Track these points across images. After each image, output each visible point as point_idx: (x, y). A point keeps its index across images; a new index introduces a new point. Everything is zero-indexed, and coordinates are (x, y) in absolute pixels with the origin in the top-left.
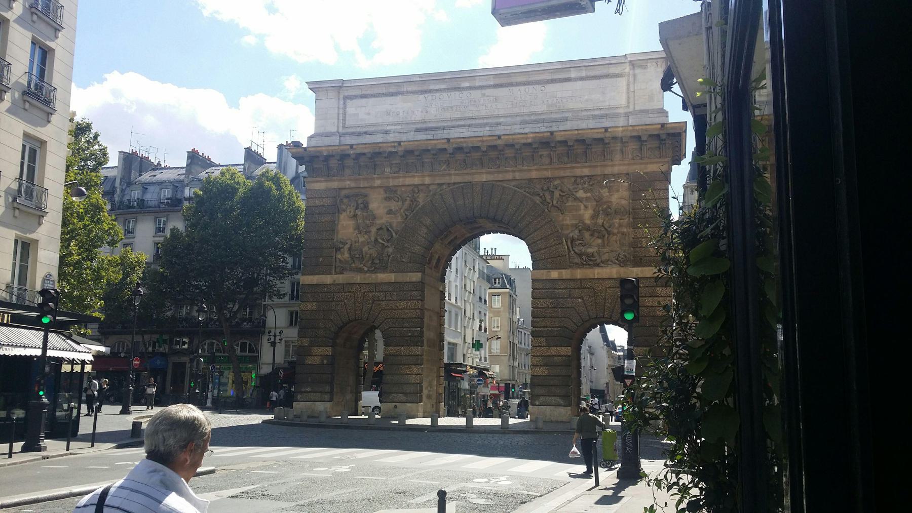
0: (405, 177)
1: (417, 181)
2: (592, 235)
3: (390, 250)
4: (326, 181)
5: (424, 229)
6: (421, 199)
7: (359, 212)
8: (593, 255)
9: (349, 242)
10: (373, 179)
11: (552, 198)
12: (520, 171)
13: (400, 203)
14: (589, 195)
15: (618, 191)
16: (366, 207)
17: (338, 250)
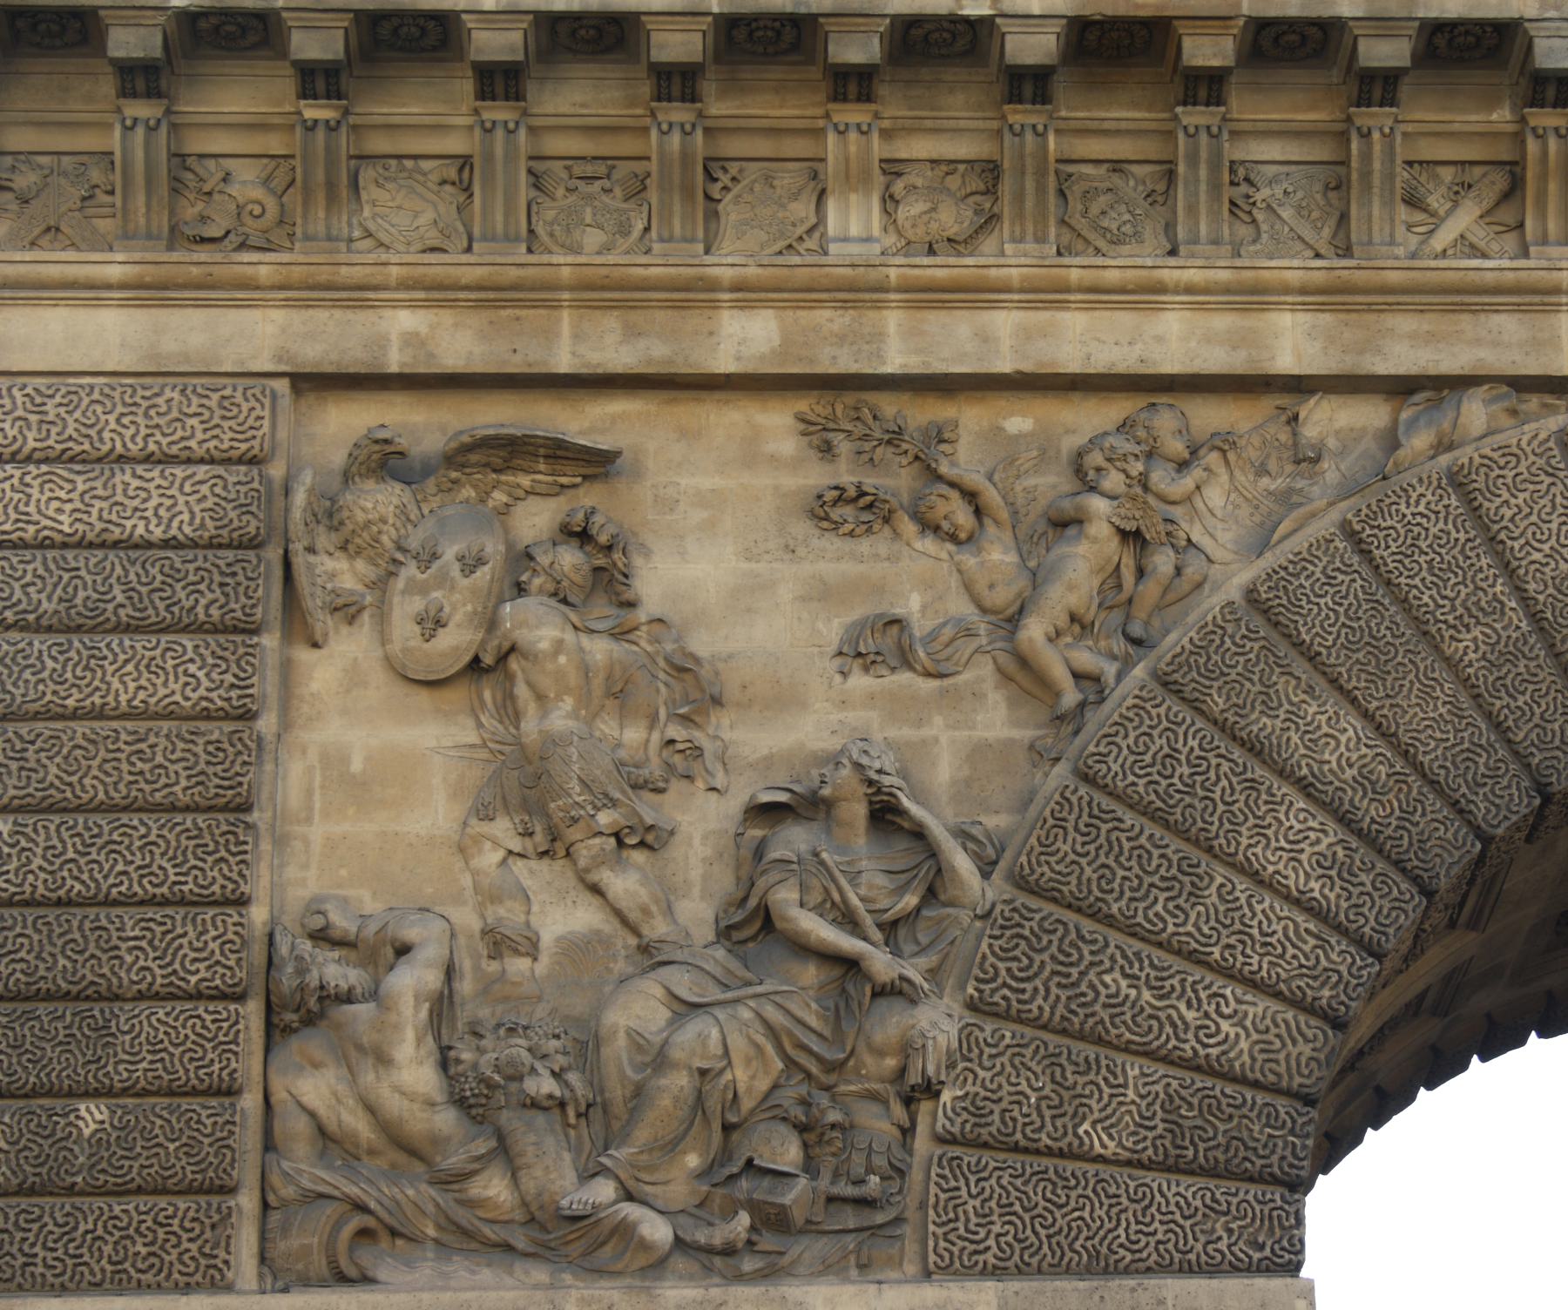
0: (1047, 294)
1: (1174, 340)
3: (938, 1023)
4: (149, 292)
5: (1296, 812)
6: (1223, 529)
7: (539, 626)
9: (428, 937)
10: (694, 294)
13: (998, 555)
16: (605, 575)
17: (297, 1014)
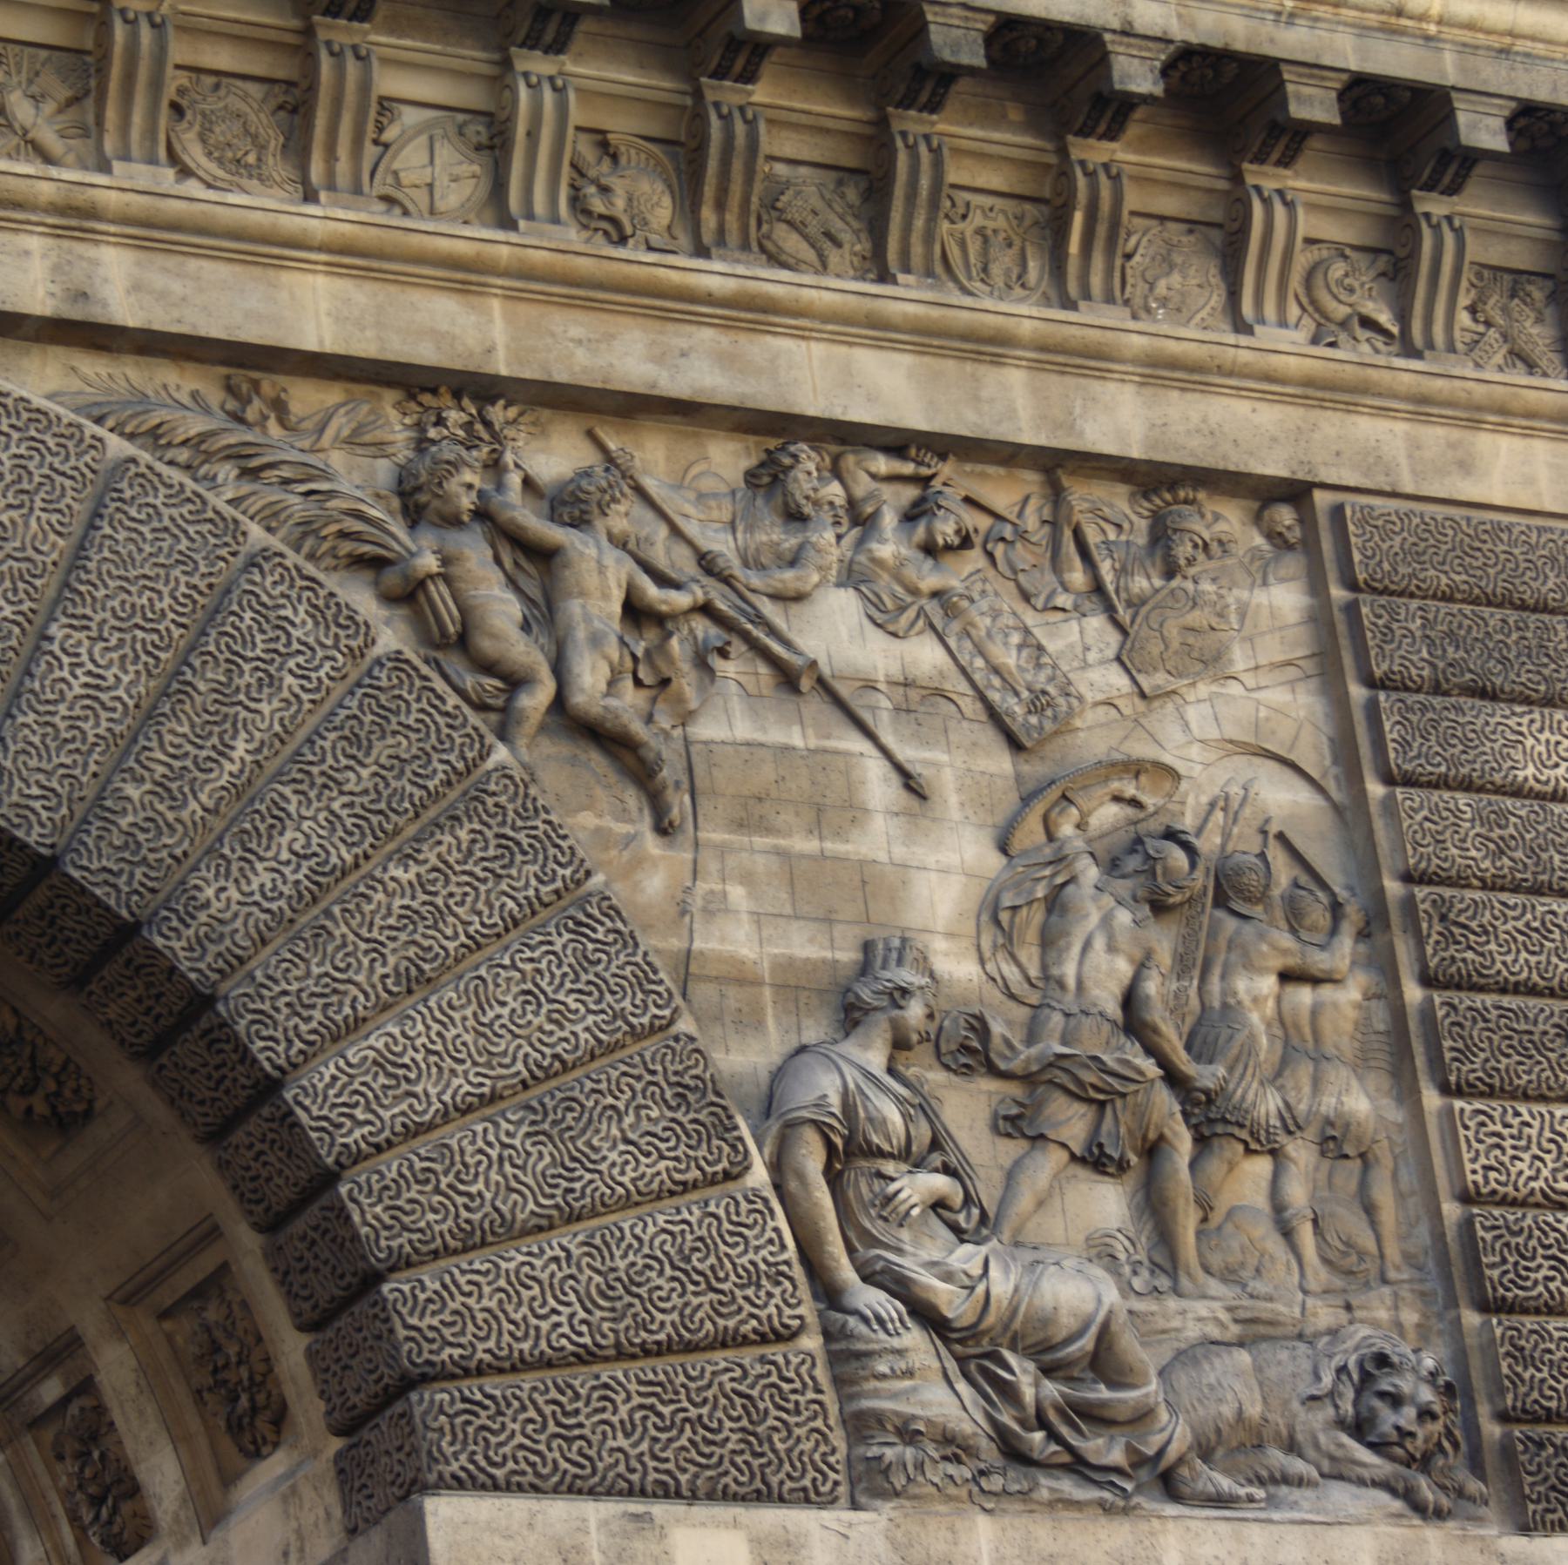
2: (1016, 1125)
8: (1104, 1361)
11: (544, 614)
12: (153, 233)
14: (926, 656)
15: (1212, 663)
